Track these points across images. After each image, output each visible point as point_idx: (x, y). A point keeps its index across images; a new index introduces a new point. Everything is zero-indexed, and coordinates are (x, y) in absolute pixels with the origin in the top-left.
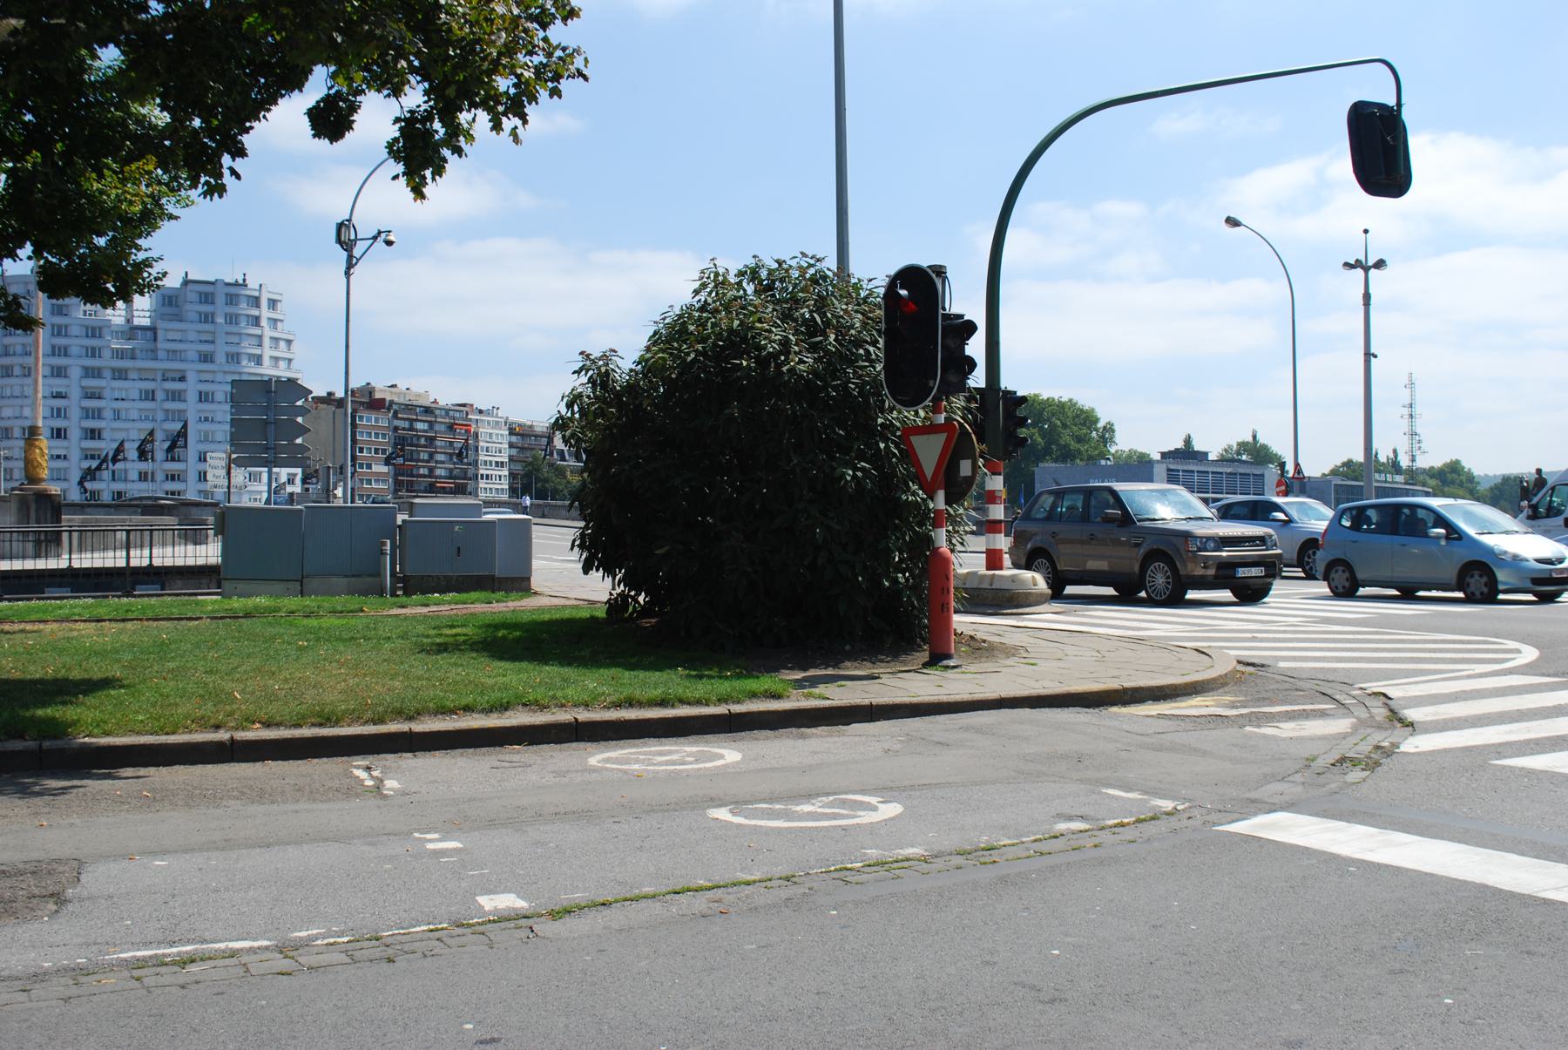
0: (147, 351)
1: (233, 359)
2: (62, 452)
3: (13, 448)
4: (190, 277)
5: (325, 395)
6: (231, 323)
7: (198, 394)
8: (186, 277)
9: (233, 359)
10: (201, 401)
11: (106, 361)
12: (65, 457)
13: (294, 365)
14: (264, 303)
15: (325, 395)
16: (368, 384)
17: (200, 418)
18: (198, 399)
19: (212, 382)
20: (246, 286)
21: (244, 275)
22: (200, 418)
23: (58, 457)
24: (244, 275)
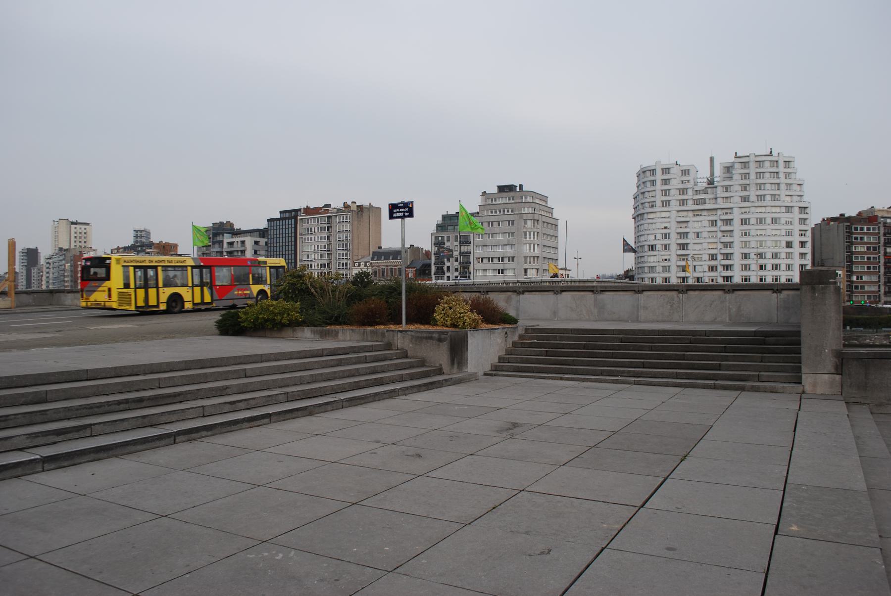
0: (712, 199)
1: (761, 198)
2: (667, 257)
3: (644, 256)
4: (738, 155)
5: (839, 216)
6: (760, 178)
7: (740, 220)
8: (736, 155)
9: (761, 198)
10: (742, 224)
11: (690, 206)
12: (669, 260)
13: (805, 198)
14: (781, 164)
15: (839, 216)
16: (872, 207)
17: (742, 233)
18: (740, 223)
19: (749, 212)
20: (772, 155)
21: (771, 149)
22: (742, 233)
23: (666, 260)
24: (771, 149)
